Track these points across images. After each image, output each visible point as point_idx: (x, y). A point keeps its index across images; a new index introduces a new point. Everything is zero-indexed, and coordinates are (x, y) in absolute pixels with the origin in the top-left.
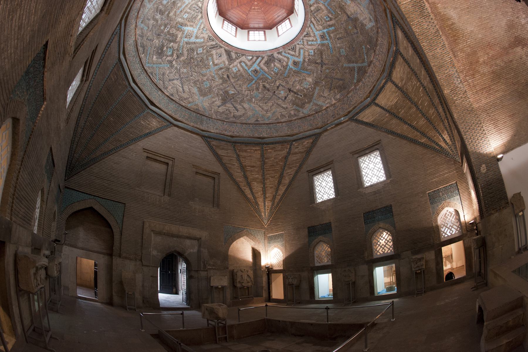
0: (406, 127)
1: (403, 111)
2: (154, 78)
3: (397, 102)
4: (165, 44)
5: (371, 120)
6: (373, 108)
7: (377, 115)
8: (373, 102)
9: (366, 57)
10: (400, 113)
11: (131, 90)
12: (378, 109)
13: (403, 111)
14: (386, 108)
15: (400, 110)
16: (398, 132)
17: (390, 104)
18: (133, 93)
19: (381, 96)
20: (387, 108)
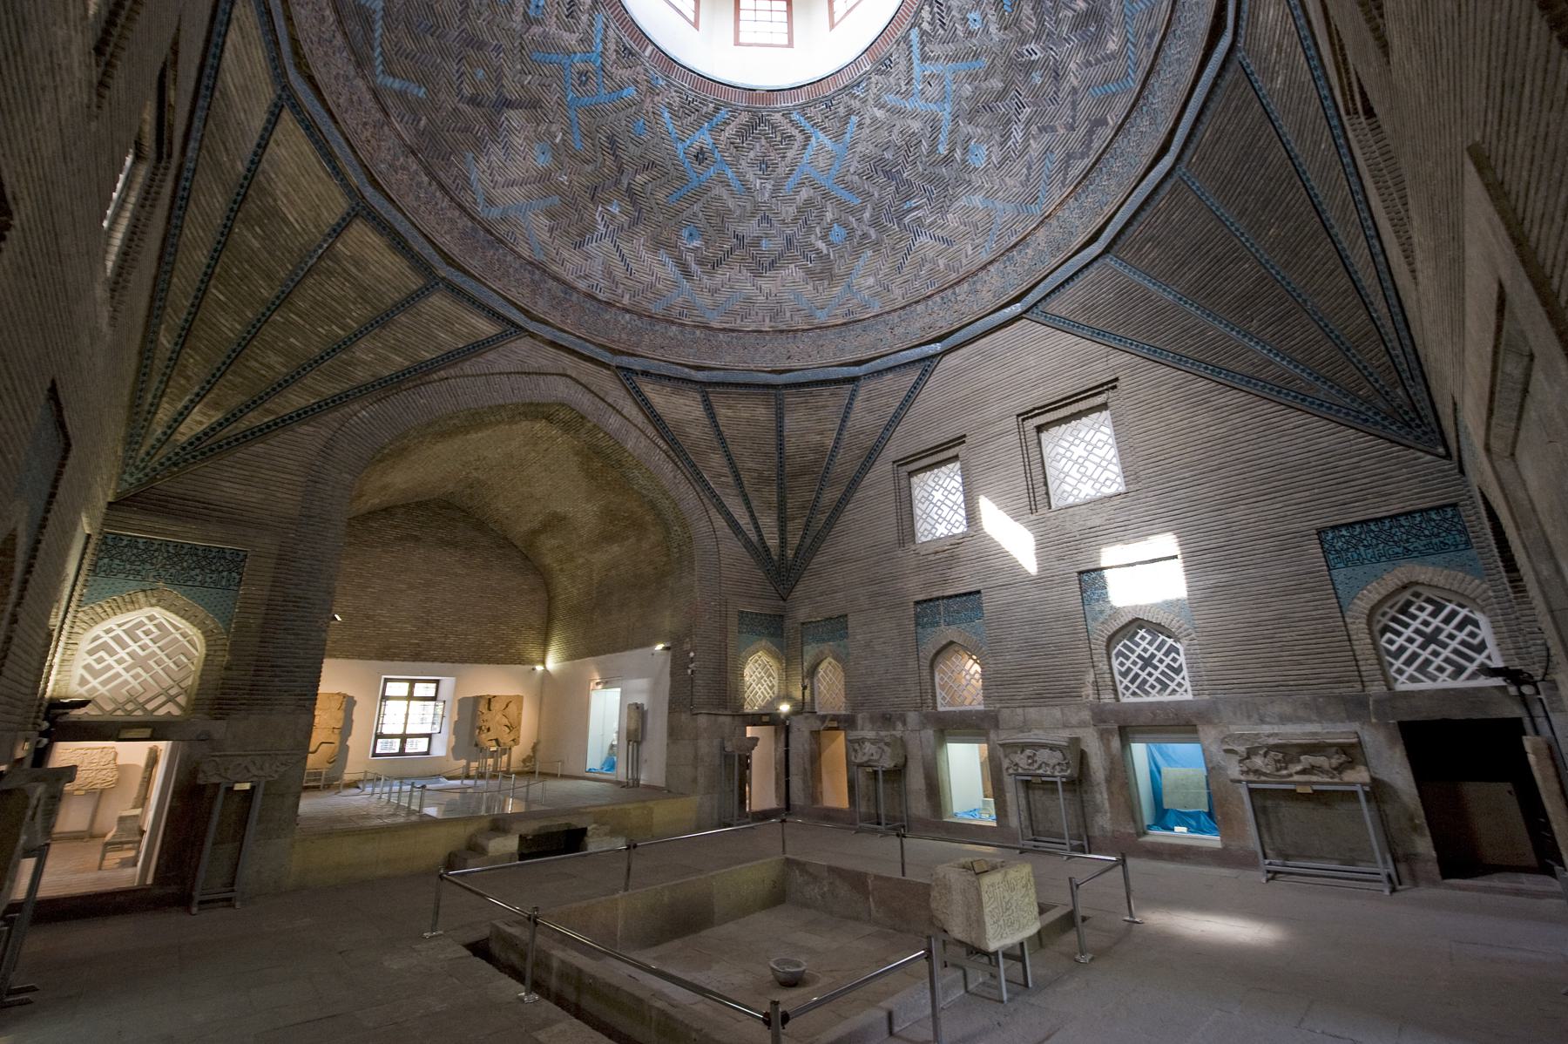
0: (201, 257)
1: (256, 244)
2: (1159, 24)
3: (285, 220)
4: (1070, 14)
5: (229, 80)
6: (267, 93)
7: (242, 115)
8: (285, 101)
9: (397, 85)
10: (248, 229)
11: (1186, 159)
12: (258, 122)
13: (256, 244)
14: (264, 165)
15: (258, 229)
16: (186, 231)
17: (280, 187)
18: (1192, 146)
19: (307, 148)
20: (263, 172)
